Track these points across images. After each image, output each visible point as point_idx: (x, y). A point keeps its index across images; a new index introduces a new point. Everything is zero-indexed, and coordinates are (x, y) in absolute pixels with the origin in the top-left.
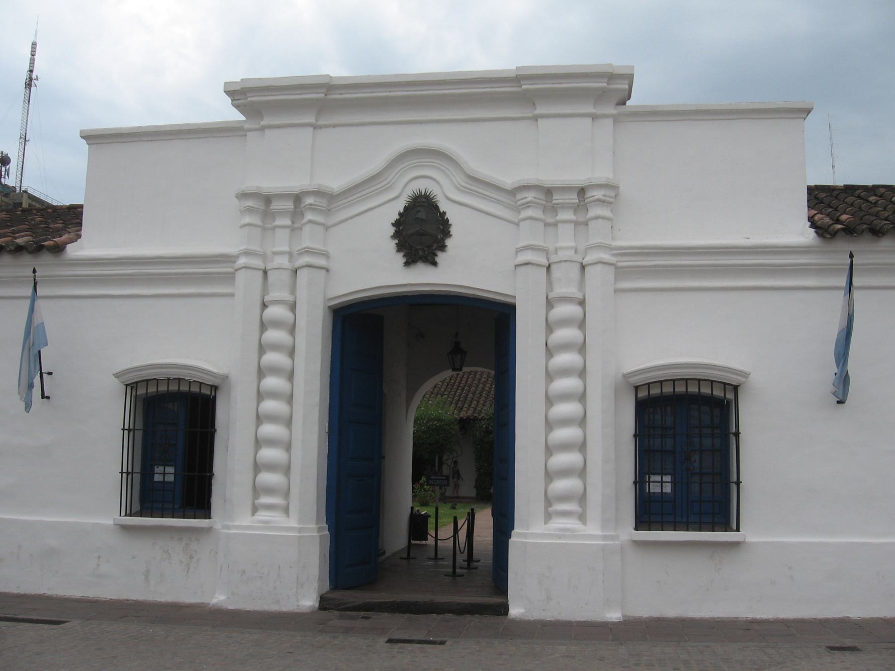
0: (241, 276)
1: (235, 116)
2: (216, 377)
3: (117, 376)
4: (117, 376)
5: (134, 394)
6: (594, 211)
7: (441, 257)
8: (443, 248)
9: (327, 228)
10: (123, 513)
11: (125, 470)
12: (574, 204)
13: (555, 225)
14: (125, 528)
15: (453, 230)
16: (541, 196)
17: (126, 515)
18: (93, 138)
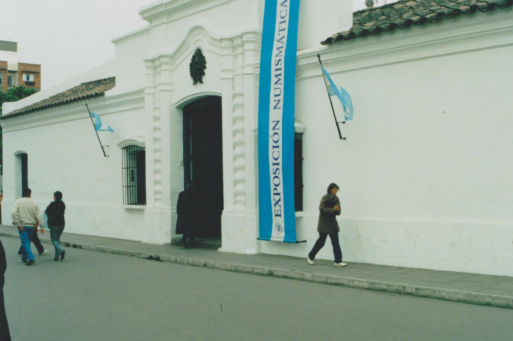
0: (147, 98)
1: (146, 23)
2: (141, 144)
3: (118, 145)
4: (118, 145)
5: (128, 152)
6: (246, 47)
7: (204, 79)
8: (204, 74)
9: (172, 71)
10: (125, 203)
11: (124, 185)
12: (240, 44)
13: (236, 56)
14: (128, 210)
15: (207, 65)
16: (229, 42)
17: (128, 204)
18: (114, 42)
